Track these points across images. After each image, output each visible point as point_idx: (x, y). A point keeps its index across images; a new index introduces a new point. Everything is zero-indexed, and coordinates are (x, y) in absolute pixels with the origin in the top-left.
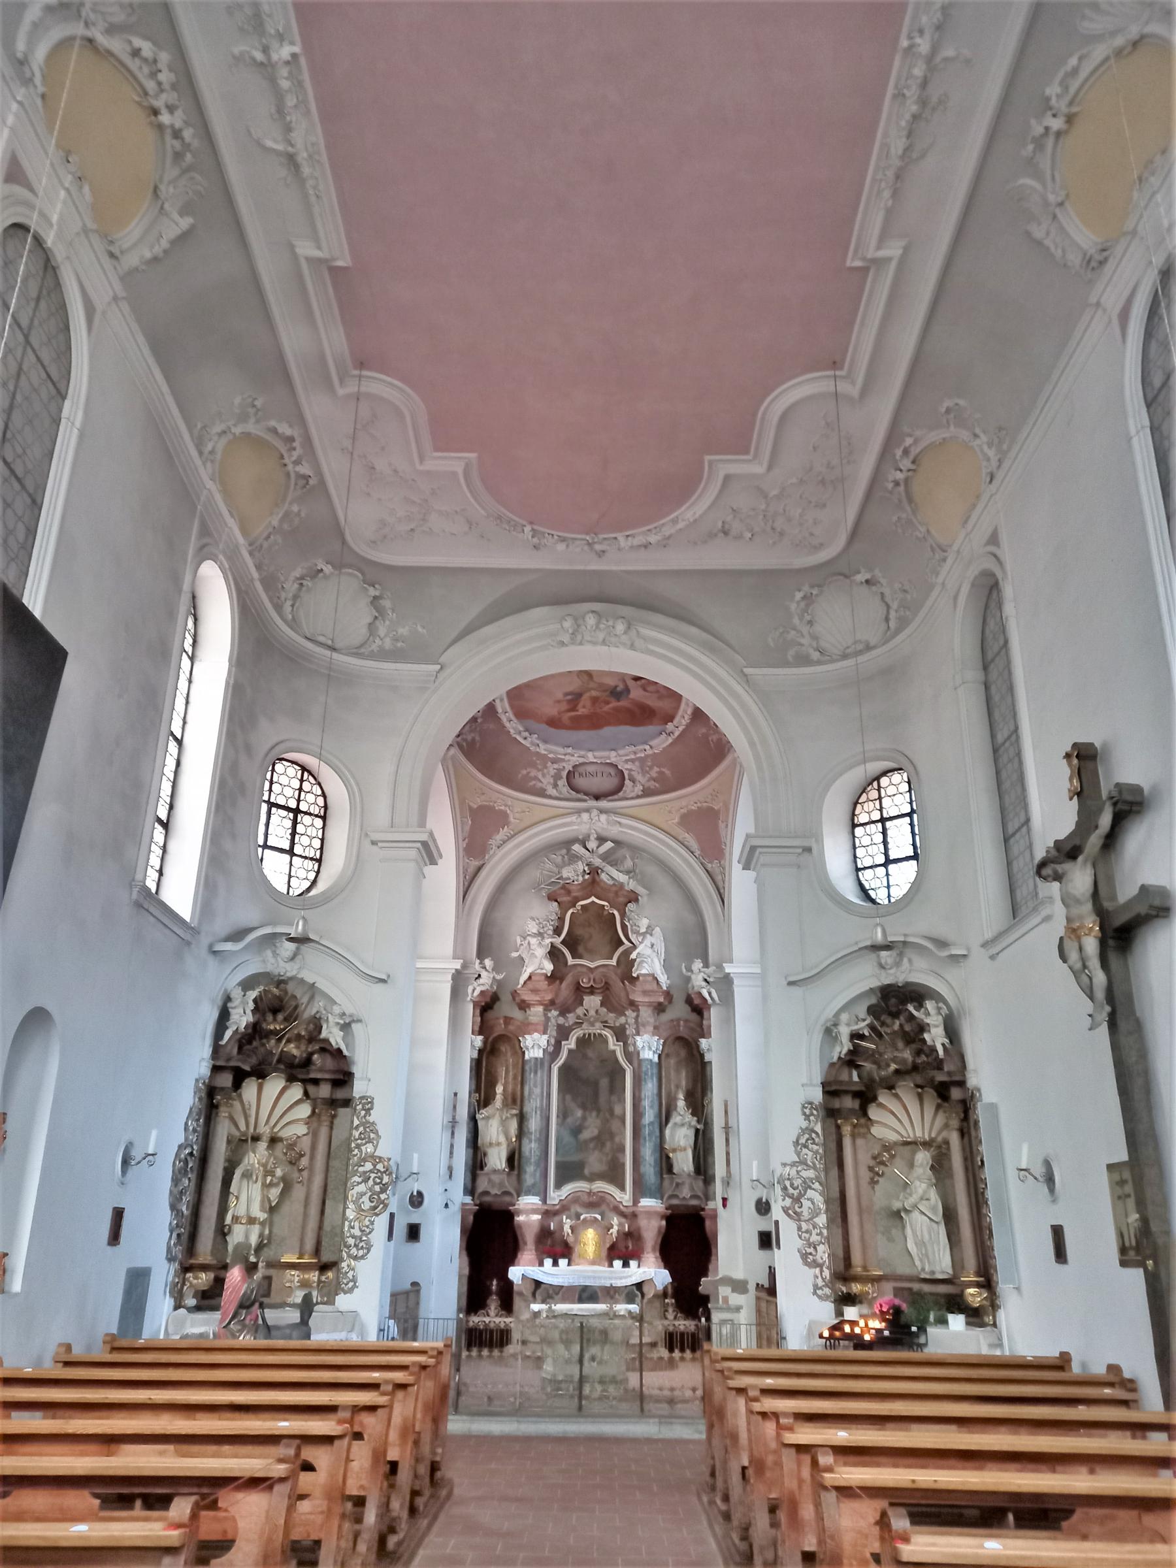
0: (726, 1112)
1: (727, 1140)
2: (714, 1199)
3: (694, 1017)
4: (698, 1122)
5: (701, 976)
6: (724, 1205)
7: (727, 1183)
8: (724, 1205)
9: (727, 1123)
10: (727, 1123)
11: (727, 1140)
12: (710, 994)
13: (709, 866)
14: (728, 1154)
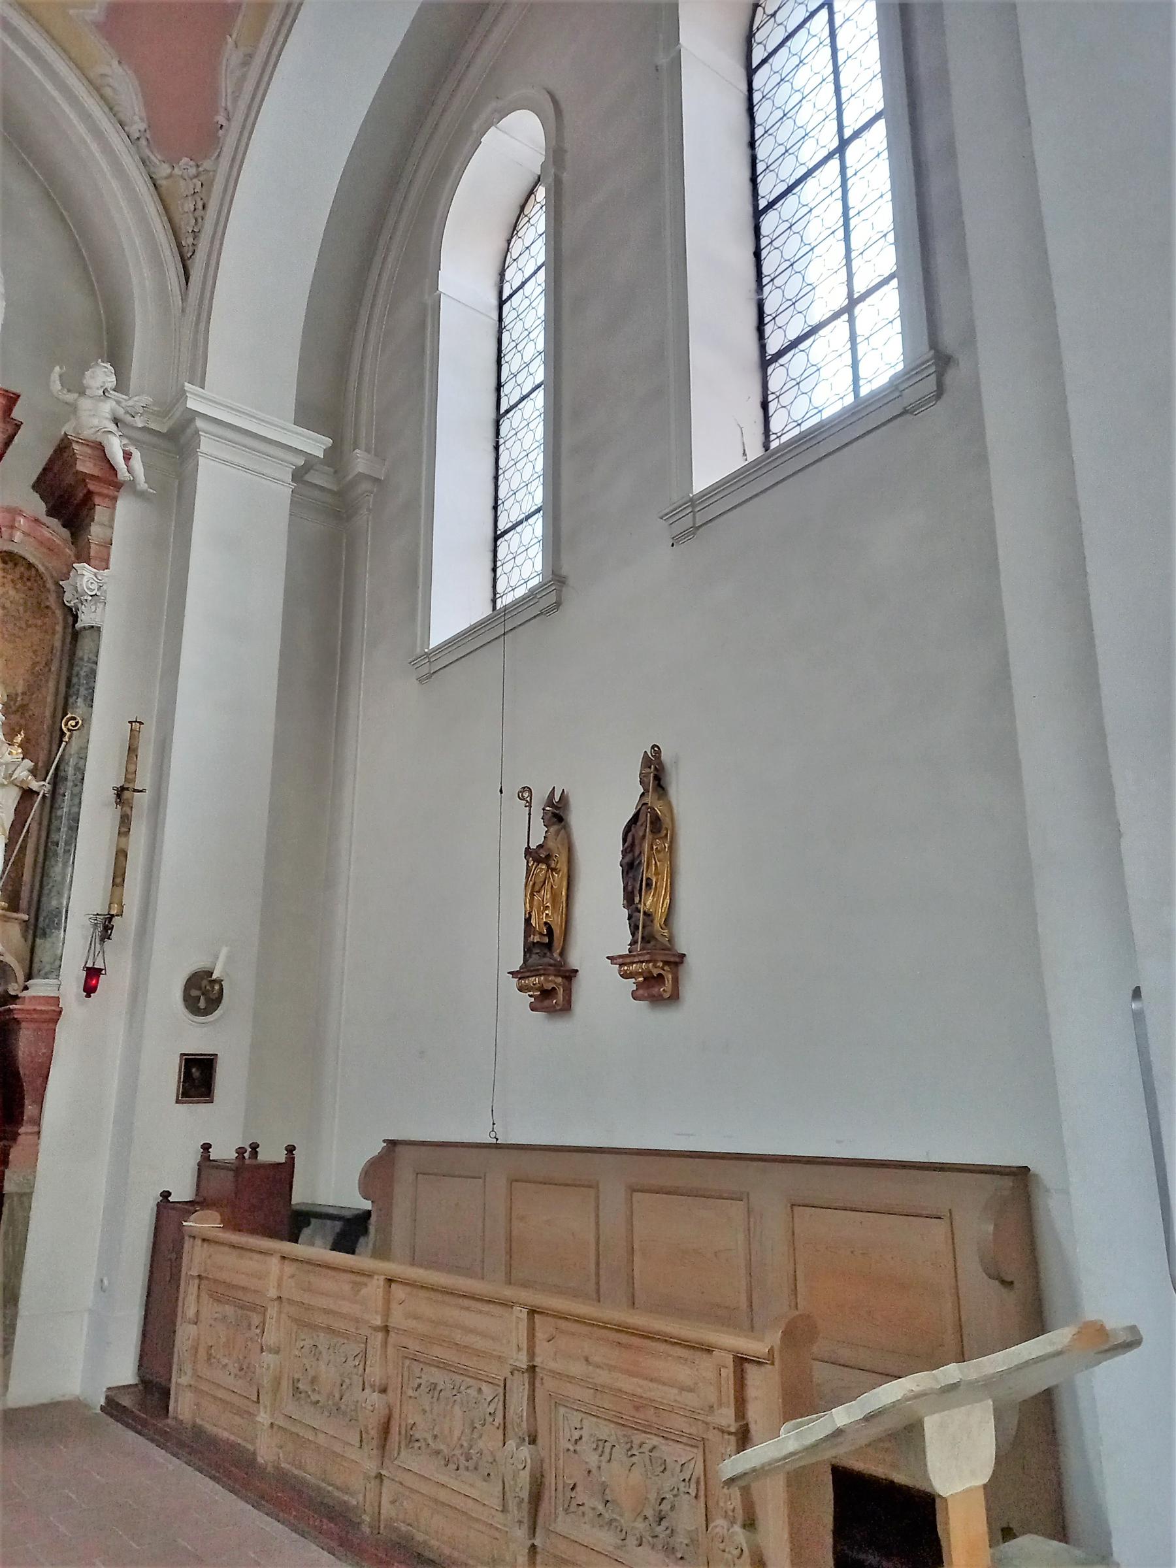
0: (132, 750)
1: (125, 822)
2: (55, 971)
3: (55, 531)
4: (33, 772)
5: (107, 407)
6: (89, 990)
7: (106, 927)
8: (89, 990)
9: (130, 775)
10: (130, 775)
11: (125, 822)
12: (127, 456)
13: (164, 170)
14: (121, 854)
